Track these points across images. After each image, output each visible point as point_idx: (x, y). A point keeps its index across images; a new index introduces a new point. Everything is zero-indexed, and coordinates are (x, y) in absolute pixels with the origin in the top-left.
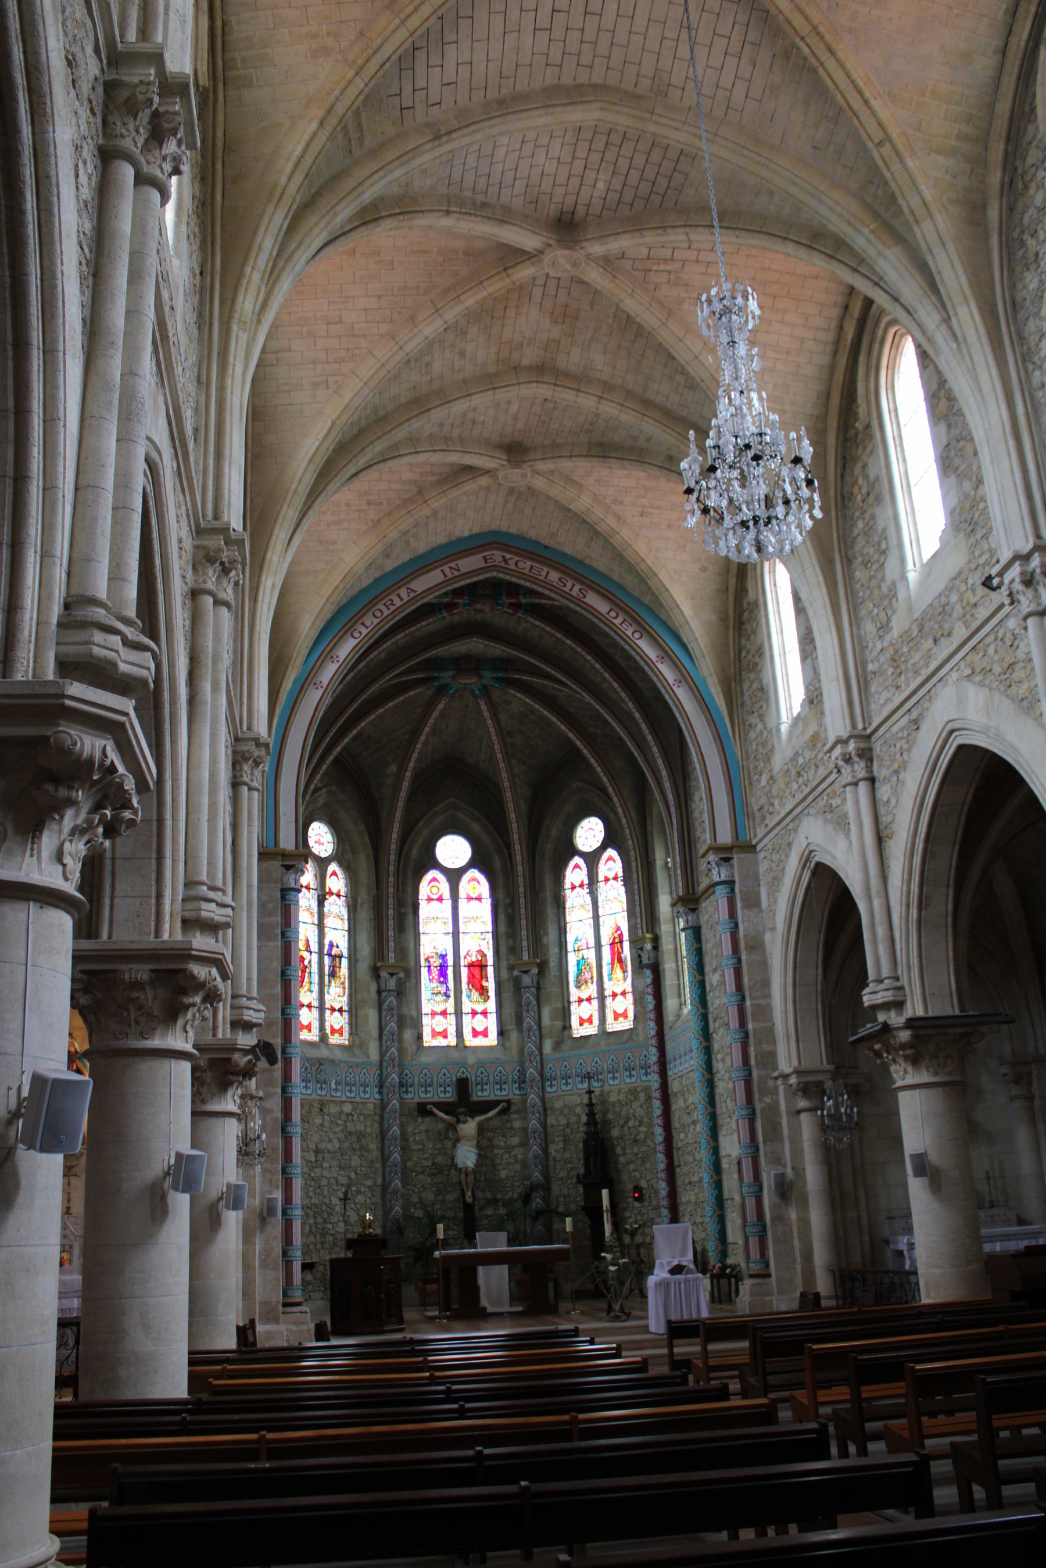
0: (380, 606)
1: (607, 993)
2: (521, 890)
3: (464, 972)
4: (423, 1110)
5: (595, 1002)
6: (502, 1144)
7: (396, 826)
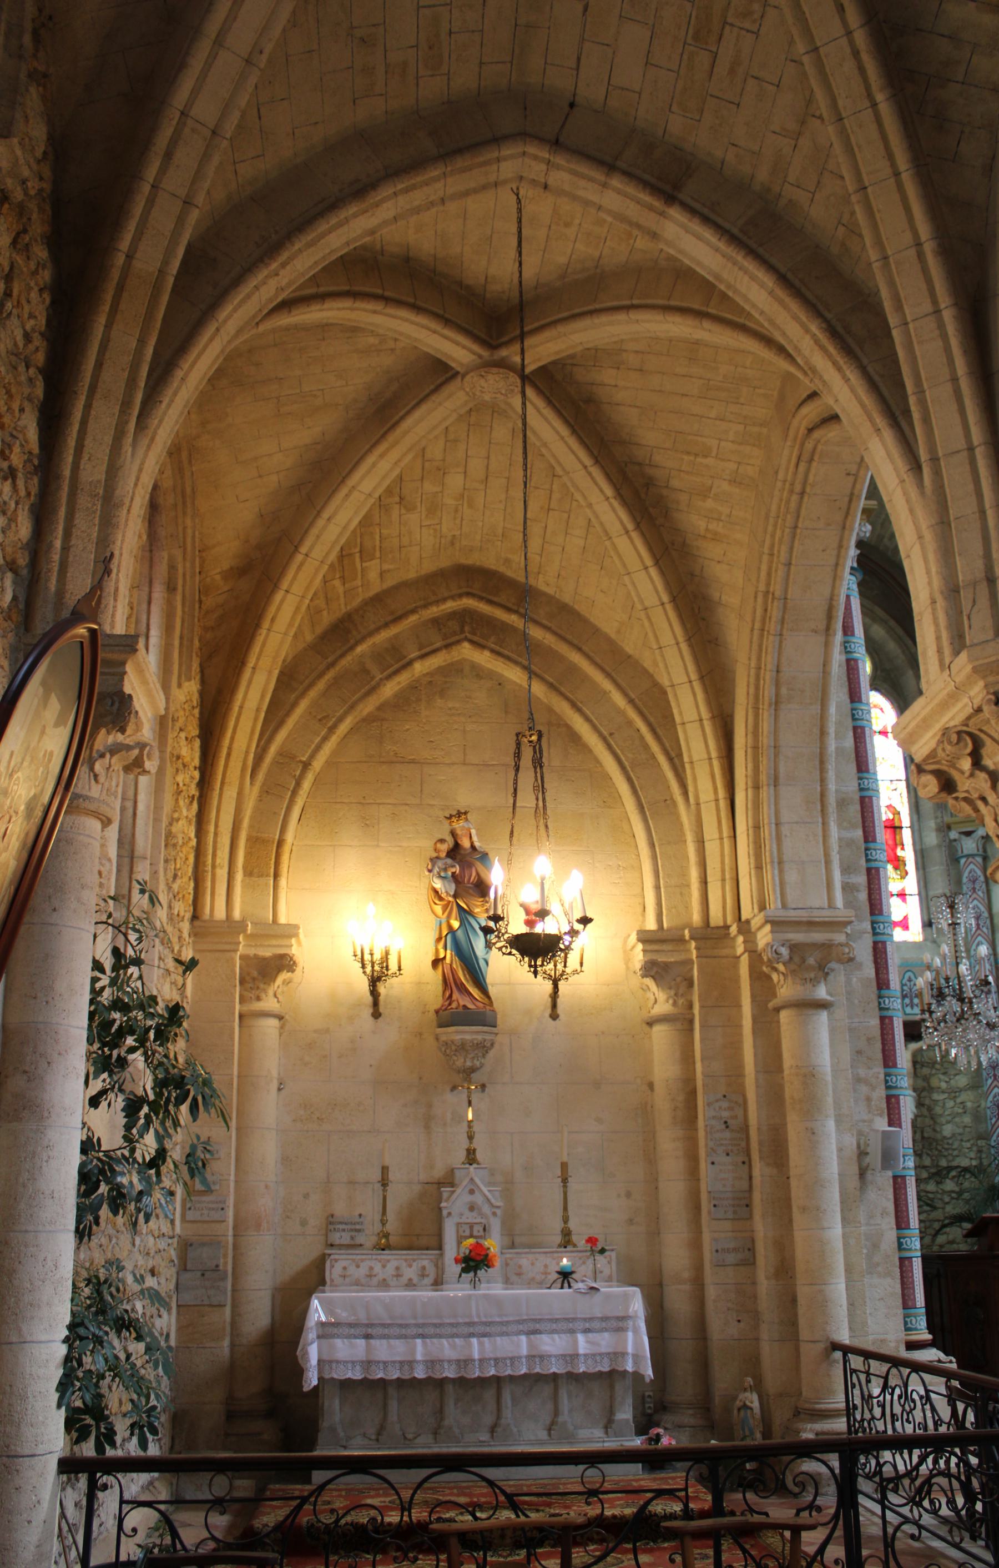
6: (944, 1085)
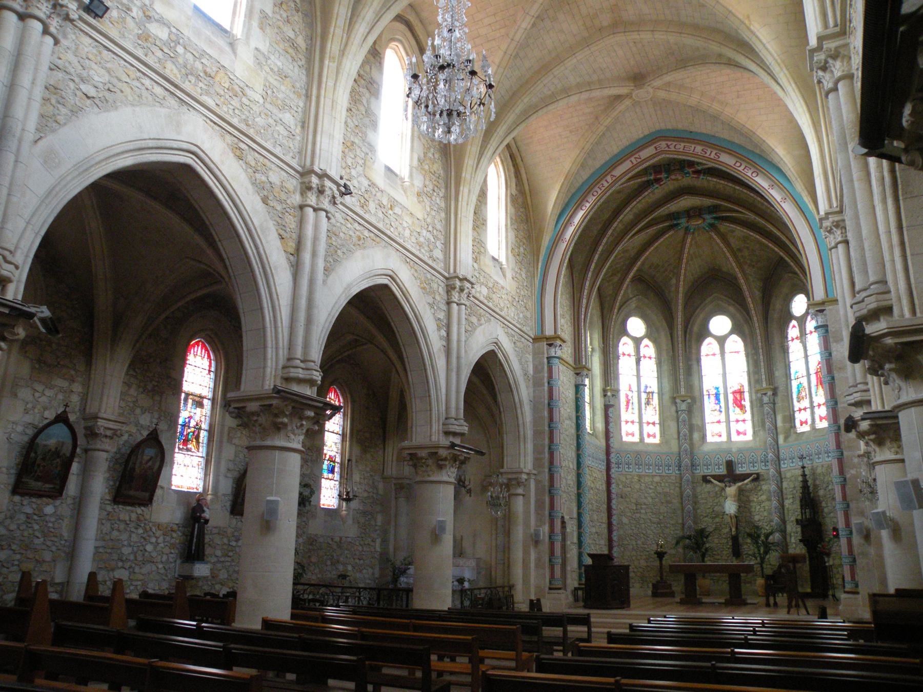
1: (815, 404)
3: (731, 397)
4: (705, 479)
5: (809, 411)
7: (680, 314)
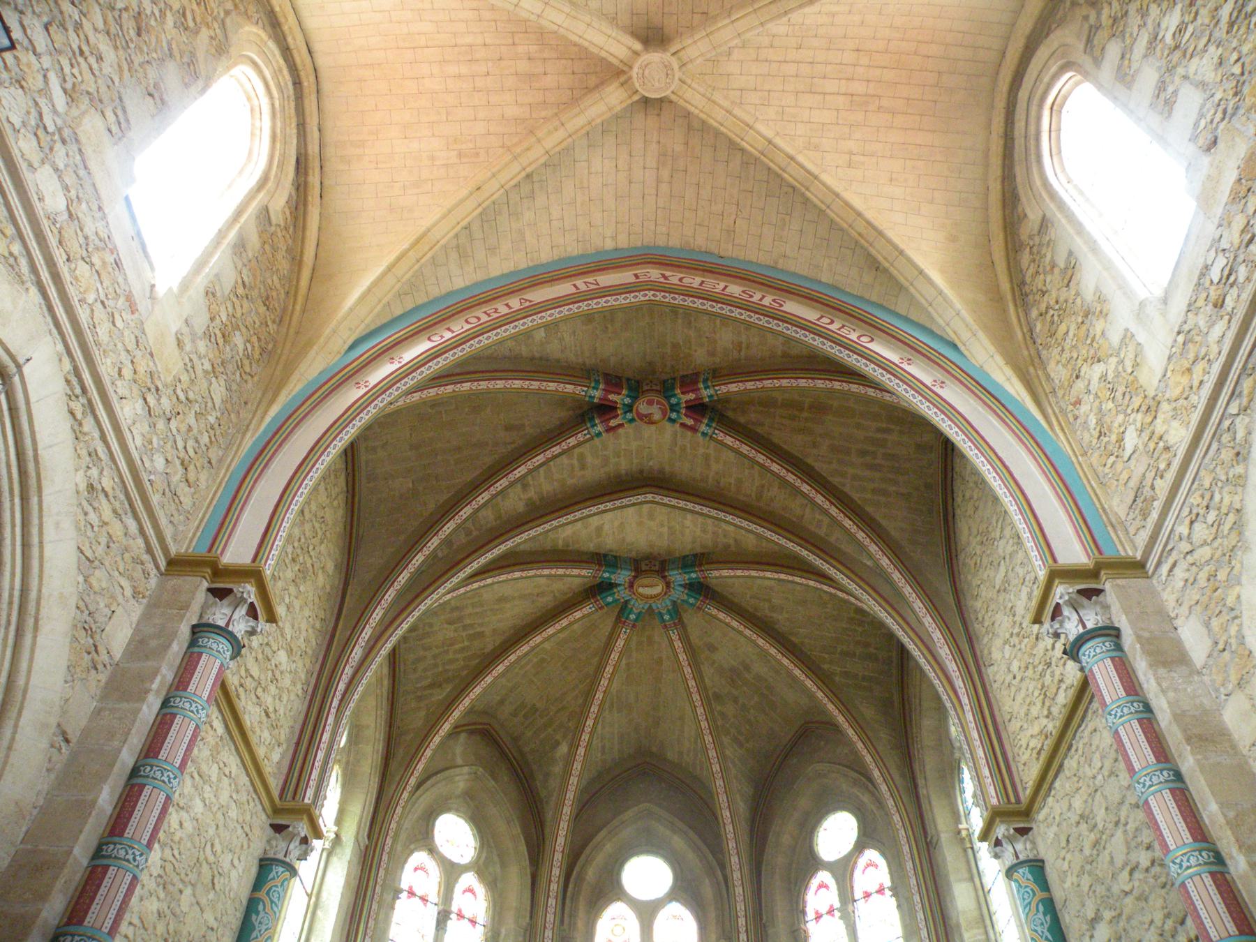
0: (479, 312)
2: (742, 921)
7: (564, 825)
